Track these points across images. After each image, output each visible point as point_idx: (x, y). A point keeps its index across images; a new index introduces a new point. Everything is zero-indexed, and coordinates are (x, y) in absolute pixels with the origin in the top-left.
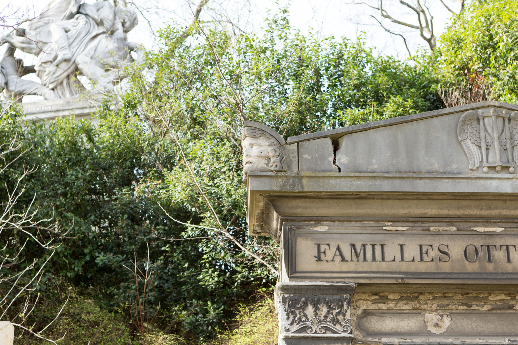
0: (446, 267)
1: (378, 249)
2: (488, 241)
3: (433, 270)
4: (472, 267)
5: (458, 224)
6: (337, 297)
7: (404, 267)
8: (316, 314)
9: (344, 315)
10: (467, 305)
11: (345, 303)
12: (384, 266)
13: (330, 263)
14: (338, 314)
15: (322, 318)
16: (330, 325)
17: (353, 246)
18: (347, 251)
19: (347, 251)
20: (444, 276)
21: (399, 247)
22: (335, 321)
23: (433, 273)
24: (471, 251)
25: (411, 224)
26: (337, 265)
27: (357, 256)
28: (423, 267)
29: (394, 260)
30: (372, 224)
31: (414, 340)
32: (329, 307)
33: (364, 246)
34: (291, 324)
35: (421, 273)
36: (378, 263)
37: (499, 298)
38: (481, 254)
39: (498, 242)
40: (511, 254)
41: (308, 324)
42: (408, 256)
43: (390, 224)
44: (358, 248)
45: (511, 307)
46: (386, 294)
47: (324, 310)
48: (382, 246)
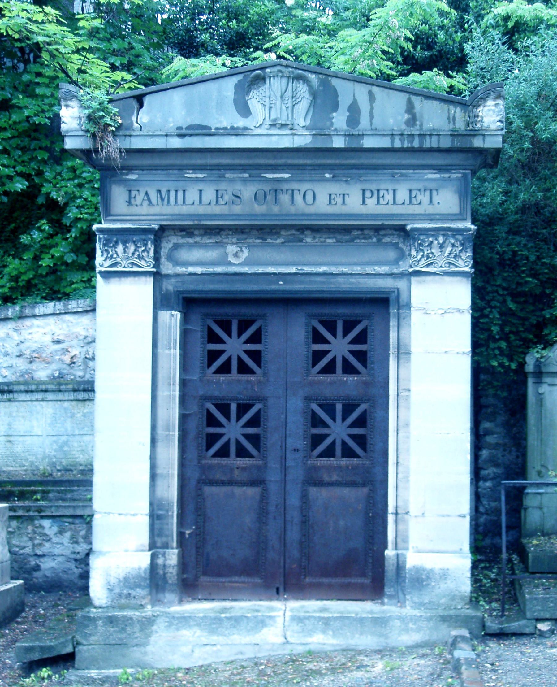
0: (237, 209)
1: (180, 194)
2: (276, 186)
3: (227, 213)
4: (259, 209)
5: (250, 171)
6: (144, 237)
7: (201, 210)
8: (125, 252)
9: (148, 252)
10: (262, 238)
11: (149, 243)
12: (185, 210)
13: (139, 207)
14: (143, 251)
15: (130, 255)
16: (136, 261)
17: (159, 191)
18: (153, 196)
19: (153, 196)
20: (234, 218)
21: (198, 192)
22: (140, 257)
23: (225, 215)
24: (261, 195)
25: (209, 172)
26: (145, 209)
27: (162, 199)
28: (217, 210)
29: (193, 204)
30: (176, 172)
31: (216, 269)
32: (136, 245)
33: (169, 191)
34: (105, 260)
35: (216, 215)
36: (180, 206)
37: (289, 233)
38: (269, 197)
39: (285, 186)
40: (295, 197)
41: (119, 260)
42: (205, 200)
43: (191, 172)
44: (164, 193)
45: (301, 241)
46: (192, 230)
47: (132, 248)
48: (184, 191)
